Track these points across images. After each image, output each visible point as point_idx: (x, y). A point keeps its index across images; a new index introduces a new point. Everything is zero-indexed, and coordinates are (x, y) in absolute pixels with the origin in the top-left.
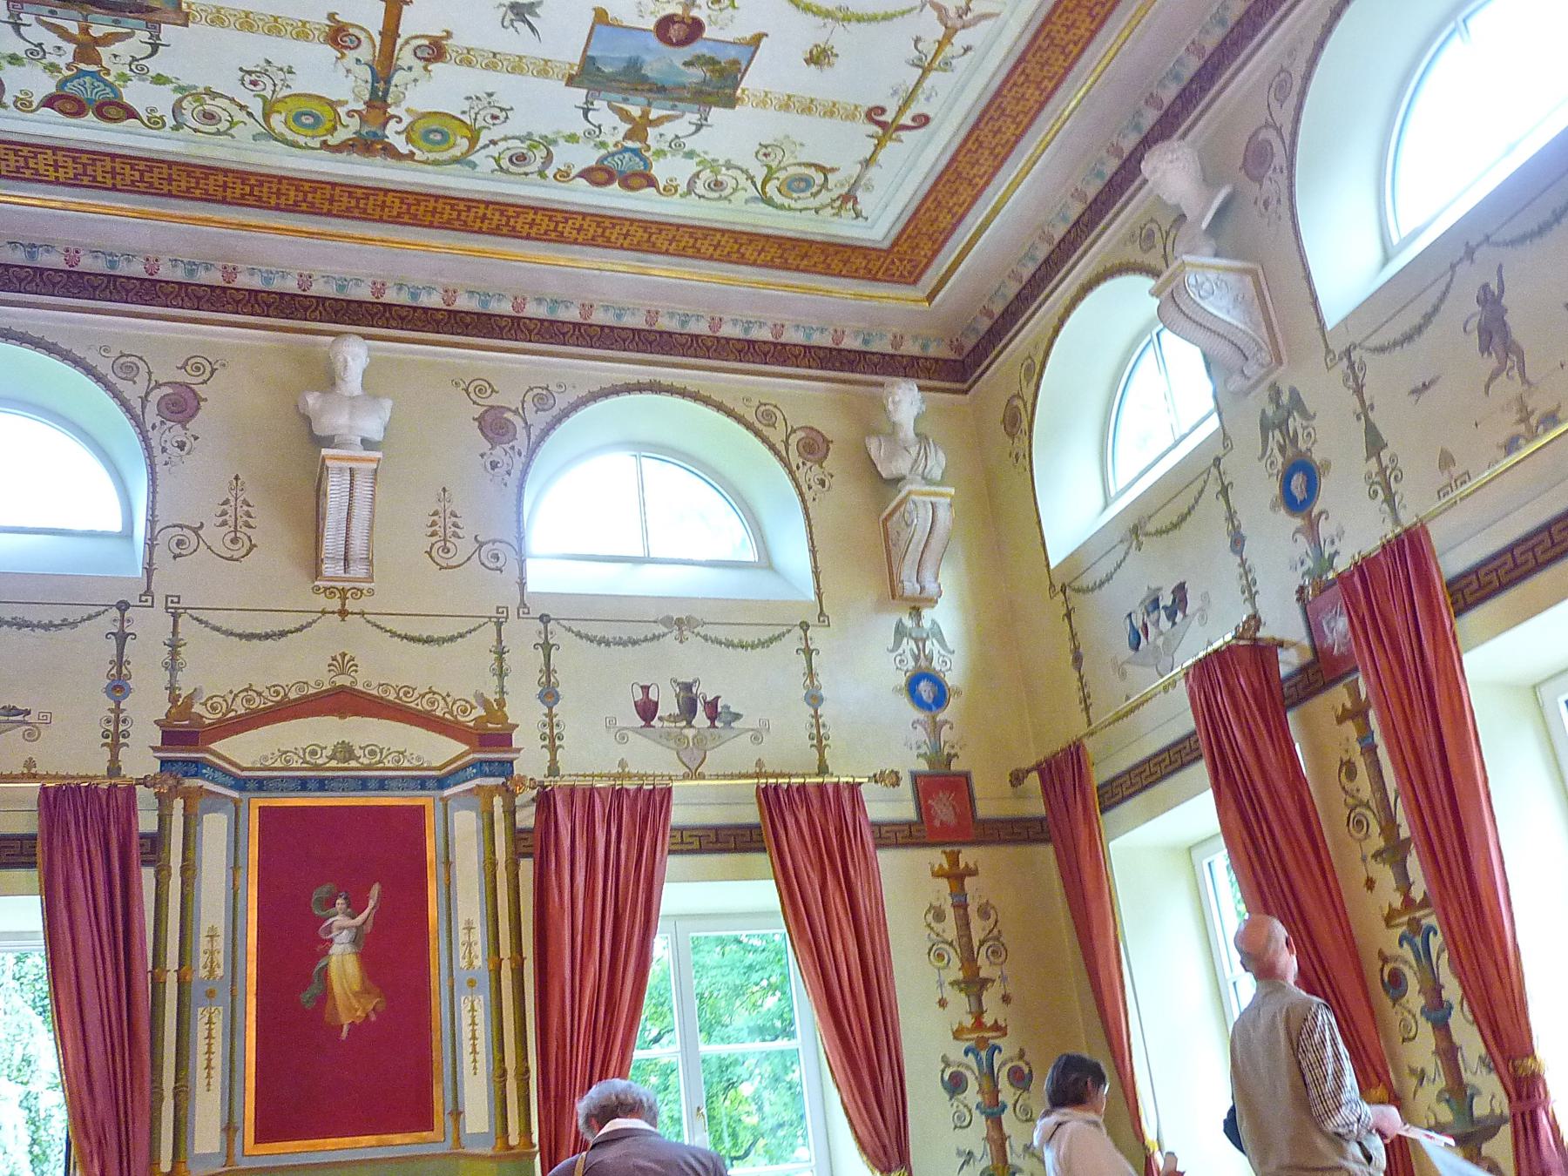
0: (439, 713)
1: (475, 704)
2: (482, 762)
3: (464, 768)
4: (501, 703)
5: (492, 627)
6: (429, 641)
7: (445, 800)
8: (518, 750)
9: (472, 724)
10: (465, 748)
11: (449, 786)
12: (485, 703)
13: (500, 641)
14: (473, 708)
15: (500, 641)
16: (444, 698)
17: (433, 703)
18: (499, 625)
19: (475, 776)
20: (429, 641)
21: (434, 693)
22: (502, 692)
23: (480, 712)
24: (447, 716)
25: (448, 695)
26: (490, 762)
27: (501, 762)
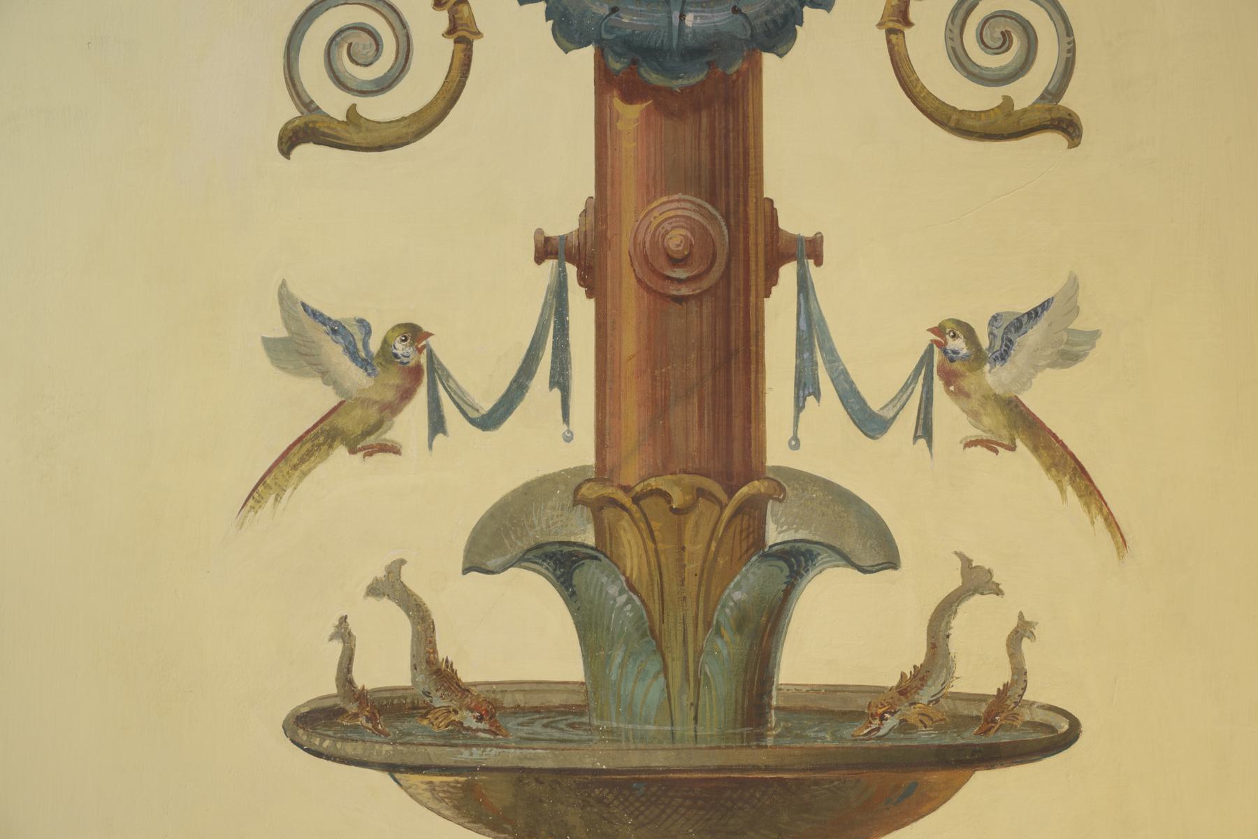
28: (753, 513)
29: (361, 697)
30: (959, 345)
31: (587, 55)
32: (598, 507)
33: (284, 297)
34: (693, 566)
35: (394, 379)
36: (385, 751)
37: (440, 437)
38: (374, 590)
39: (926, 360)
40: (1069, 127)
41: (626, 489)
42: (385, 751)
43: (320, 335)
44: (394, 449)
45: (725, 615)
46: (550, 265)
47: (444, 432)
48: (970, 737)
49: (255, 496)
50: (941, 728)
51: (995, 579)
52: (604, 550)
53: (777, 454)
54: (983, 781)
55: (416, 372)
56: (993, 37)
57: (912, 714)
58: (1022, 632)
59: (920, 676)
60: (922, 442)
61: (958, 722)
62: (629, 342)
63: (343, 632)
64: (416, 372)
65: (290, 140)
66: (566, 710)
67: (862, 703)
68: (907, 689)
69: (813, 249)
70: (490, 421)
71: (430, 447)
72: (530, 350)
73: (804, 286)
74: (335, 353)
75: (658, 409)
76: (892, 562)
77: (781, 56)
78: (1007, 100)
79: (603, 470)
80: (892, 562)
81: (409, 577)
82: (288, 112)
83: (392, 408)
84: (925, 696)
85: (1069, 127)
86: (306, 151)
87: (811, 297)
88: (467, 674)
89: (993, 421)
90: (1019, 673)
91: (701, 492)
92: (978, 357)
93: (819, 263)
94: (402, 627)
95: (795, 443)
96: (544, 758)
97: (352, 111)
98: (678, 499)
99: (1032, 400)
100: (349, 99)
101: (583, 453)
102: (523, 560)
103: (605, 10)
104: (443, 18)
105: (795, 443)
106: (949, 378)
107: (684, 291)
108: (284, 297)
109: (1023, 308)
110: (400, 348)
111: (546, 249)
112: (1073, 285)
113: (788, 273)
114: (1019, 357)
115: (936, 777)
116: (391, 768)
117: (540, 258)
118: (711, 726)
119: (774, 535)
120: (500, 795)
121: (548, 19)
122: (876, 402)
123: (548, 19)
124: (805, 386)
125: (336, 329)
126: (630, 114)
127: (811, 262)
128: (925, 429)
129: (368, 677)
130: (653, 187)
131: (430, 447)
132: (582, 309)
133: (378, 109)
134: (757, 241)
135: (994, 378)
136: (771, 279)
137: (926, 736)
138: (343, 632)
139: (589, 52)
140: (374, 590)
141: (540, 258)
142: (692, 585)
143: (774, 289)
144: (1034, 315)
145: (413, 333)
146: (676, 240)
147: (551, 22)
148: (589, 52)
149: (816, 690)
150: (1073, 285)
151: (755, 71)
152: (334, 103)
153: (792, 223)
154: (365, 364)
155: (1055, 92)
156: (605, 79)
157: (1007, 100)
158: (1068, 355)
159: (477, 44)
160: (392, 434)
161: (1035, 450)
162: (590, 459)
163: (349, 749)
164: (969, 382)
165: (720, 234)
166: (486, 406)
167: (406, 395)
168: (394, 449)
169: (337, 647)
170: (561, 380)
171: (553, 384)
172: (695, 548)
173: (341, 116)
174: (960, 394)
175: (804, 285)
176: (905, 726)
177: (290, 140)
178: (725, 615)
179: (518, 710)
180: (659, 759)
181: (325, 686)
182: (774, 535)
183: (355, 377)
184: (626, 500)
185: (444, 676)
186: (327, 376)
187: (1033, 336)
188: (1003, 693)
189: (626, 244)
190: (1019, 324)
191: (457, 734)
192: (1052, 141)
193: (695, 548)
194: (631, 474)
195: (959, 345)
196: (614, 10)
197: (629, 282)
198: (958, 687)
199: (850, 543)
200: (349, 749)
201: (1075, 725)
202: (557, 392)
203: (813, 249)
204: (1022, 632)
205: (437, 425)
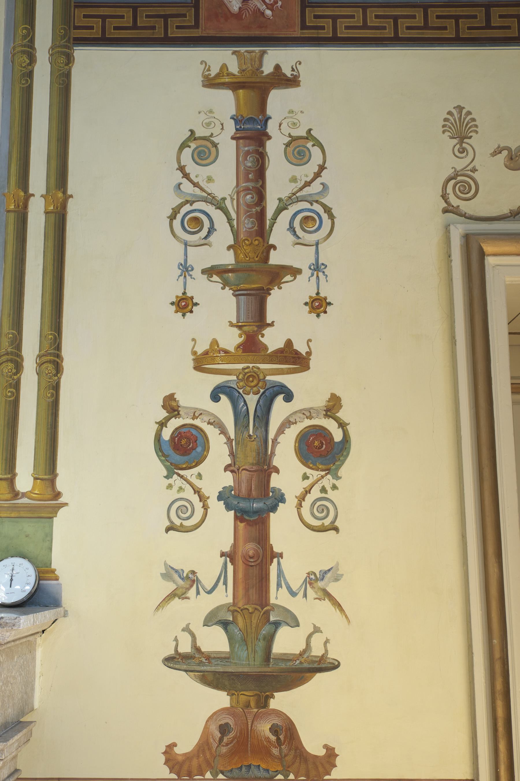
28: (267, 614)
29: (180, 654)
30: (313, 577)
31: (232, 512)
32: (233, 612)
33: (165, 564)
34: (254, 626)
35: (189, 582)
36: (185, 667)
37: (199, 595)
38: (183, 630)
39: (305, 580)
40: (336, 529)
41: (239, 608)
42: (185, 667)
43: (173, 572)
44: (188, 598)
45: (261, 637)
46: (223, 558)
47: (200, 595)
48: (316, 665)
49: (157, 608)
50: (309, 663)
51: (321, 629)
52: (234, 622)
53: (273, 600)
54: (319, 676)
55: (193, 581)
56: (320, 510)
57: (303, 660)
58: (327, 641)
59: (305, 651)
60: (305, 598)
61: (314, 662)
62: (240, 575)
63: (176, 640)
64: (193, 581)
65: (168, 530)
66: (225, 658)
67: (291, 657)
68: (301, 654)
69: (281, 555)
70: (210, 592)
71: (196, 598)
72: (219, 576)
73: (279, 563)
74: (176, 577)
75: (247, 590)
76: (298, 625)
77: (274, 513)
78: (323, 523)
79: (234, 604)
80: (298, 625)
81: (191, 627)
82: (168, 524)
83: (188, 589)
84: (305, 656)
85: (336, 529)
86: (171, 532)
87: (280, 566)
88: (203, 650)
89: (320, 594)
90: (326, 651)
91: (256, 609)
92: (317, 580)
93: (282, 558)
94: (189, 638)
95: (277, 598)
96: (220, 669)
97: (181, 523)
98: (251, 610)
99: (329, 589)
100: (180, 521)
101: (230, 600)
102: (216, 624)
103: (236, 503)
104: (201, 504)
105: (277, 598)
106: (311, 584)
107: (253, 564)
108: (165, 564)
109: (327, 569)
110: (190, 576)
111: (223, 554)
112: (338, 564)
113: (275, 560)
114: (326, 580)
115: (308, 675)
116: (186, 671)
117: (221, 557)
118: (257, 663)
119: (272, 619)
120: (210, 677)
121: (222, 488)
122: (294, 589)
123: (222, 488)
124: (279, 585)
125: (176, 571)
126: (241, 525)
127: (280, 558)
128: (305, 595)
129: (181, 650)
130: (246, 541)
131: (196, 598)
132: (230, 568)
133: (187, 523)
134: (269, 553)
135: (320, 584)
136: (272, 562)
137: (306, 665)
138: (176, 640)
139: (233, 512)
140: (183, 630)
141: (221, 557)
142: (254, 629)
143: (272, 564)
144: (329, 570)
145: (193, 572)
146: (251, 553)
147: (225, 505)
148: (233, 512)
149: (281, 654)
150: (338, 564)
151: (269, 516)
152: (177, 522)
153: (276, 549)
154: (183, 579)
155: (333, 522)
156: (236, 518)
157: (323, 523)
158: (337, 580)
159: (209, 510)
160: (188, 595)
161: (329, 600)
162: (231, 601)
163: (176, 666)
164: (315, 585)
165: (261, 552)
166: (209, 589)
167: (191, 586)
168: (188, 598)
169: (175, 643)
170: (225, 583)
171: (223, 584)
172: (254, 621)
173: (179, 525)
174: (313, 588)
175: (279, 563)
176: (301, 663)
177: (168, 530)
178: (261, 637)
179: (214, 658)
180: (246, 670)
181: (171, 652)
182: (272, 619)
183: (180, 582)
184: (239, 610)
185: (198, 650)
186: (174, 581)
187: (329, 575)
188: (323, 656)
189: (240, 554)
190: (326, 572)
191: (201, 663)
192: (333, 532)
193: (254, 621)
194: (240, 604)
195: (313, 577)
196: (238, 503)
197: (241, 562)
198: (313, 654)
199: (289, 621)
200: (176, 666)
201: (339, 663)
202: (224, 586)
203: (281, 555)
204: (327, 641)
205: (198, 593)
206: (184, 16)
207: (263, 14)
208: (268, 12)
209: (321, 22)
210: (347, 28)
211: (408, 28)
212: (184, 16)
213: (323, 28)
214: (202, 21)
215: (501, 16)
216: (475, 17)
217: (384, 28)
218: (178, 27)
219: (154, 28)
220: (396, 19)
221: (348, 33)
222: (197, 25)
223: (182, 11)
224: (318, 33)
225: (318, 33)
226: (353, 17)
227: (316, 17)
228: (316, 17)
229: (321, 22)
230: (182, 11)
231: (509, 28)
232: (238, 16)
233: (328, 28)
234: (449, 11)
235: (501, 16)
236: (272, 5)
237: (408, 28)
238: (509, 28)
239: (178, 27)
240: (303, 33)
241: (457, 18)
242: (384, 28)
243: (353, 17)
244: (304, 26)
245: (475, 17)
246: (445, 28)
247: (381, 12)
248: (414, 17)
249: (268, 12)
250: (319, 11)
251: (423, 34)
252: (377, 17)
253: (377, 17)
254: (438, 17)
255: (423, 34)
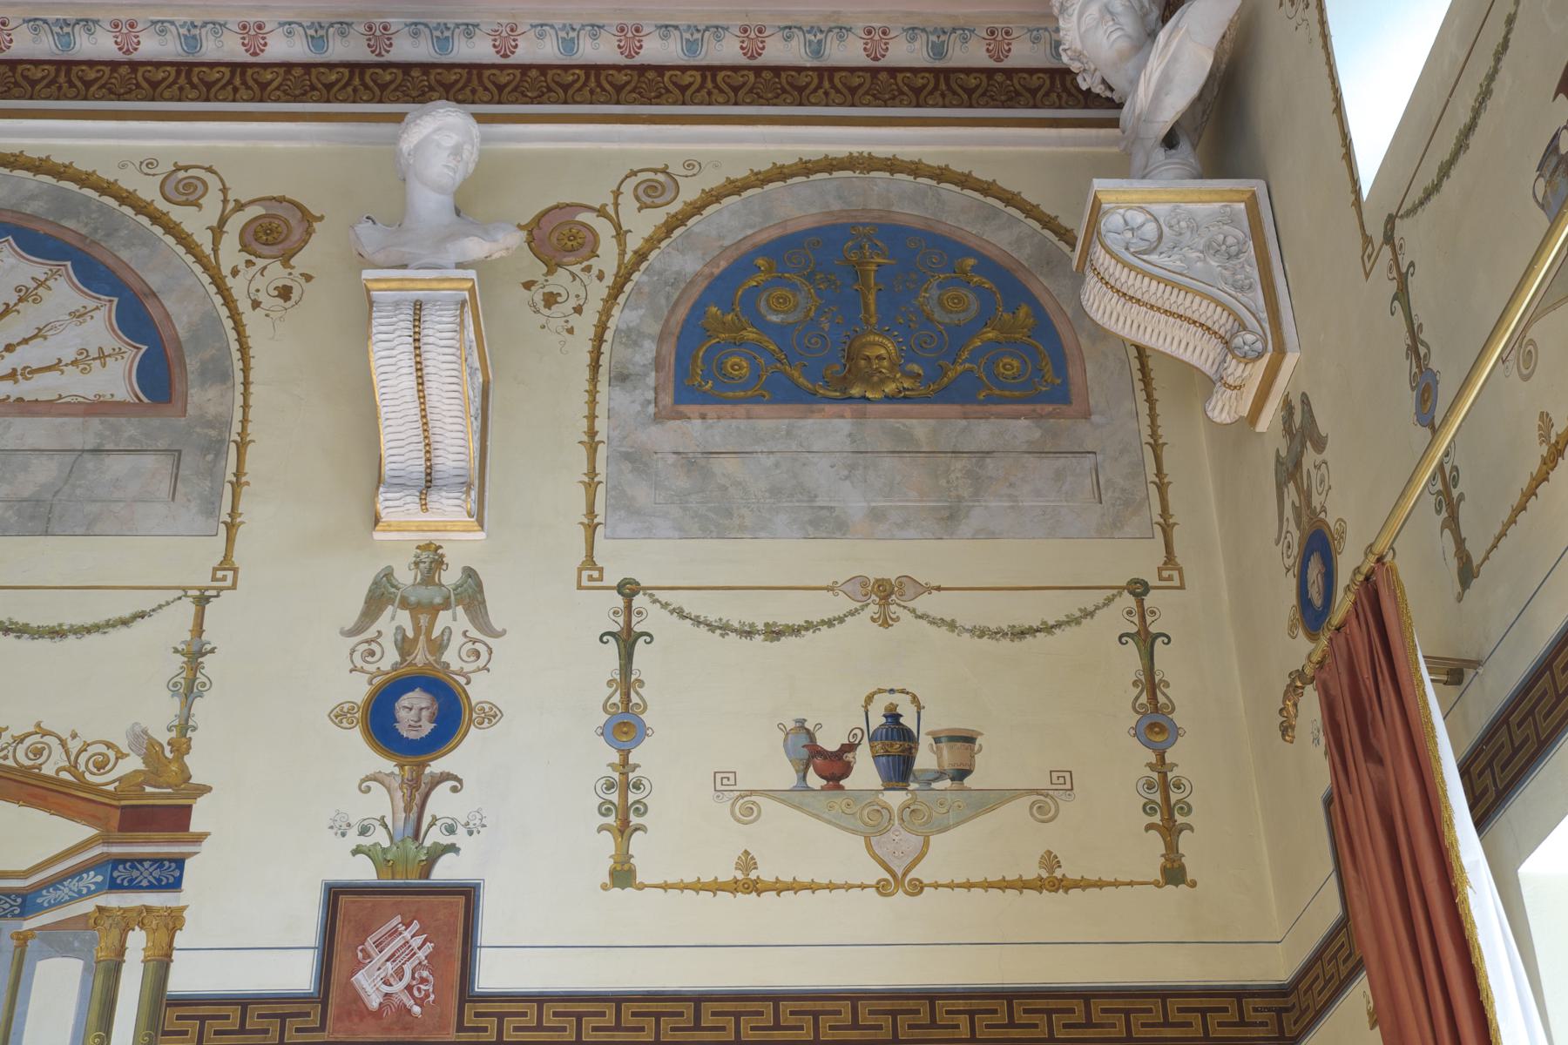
0: (49, 770)
1: (125, 750)
2: (117, 862)
3: (76, 873)
4: (181, 746)
5: (188, 608)
6: (57, 633)
7: (23, 939)
8: (199, 838)
9: (111, 788)
10: (86, 832)
11: (40, 909)
12: (151, 750)
13: (199, 629)
14: (121, 756)
15: (199, 629)
16: (63, 743)
17: (38, 753)
18: (202, 601)
19: (99, 889)
20: (57, 633)
21: (46, 733)
22: (184, 727)
23: (134, 763)
24: (65, 776)
25: (74, 736)
26: (136, 861)
27: (158, 861)
206: (308, 1015)
207: (409, 1011)
208: (417, 1009)
209: (483, 1022)
210: (516, 1029)
211: (595, 1029)
212: (308, 1015)
213: (485, 1029)
214: (330, 1023)
215: (714, 1014)
216: (681, 1014)
217: (564, 1029)
218: (298, 1030)
219: (266, 1031)
220: (579, 1017)
221: (517, 1036)
222: (322, 1028)
223: (306, 1008)
224: (478, 1037)
225: (478, 1037)
226: (524, 1014)
227: (477, 1015)
228: (477, 1015)
229: (483, 1022)
230: (306, 1008)
231: (723, 1029)
232: (378, 1014)
233: (492, 1030)
234: (648, 1007)
235: (714, 1014)
236: (422, 999)
237: (595, 1029)
238: (723, 1029)
239: (298, 1030)
240: (458, 1037)
241: (658, 1016)
242: (564, 1029)
243: (524, 1014)
244: (461, 1028)
245: (681, 1014)
246: (642, 1029)
247: (560, 1008)
248: (603, 1014)
249: (417, 1009)
250: (482, 1007)
251: (613, 1036)
252: (556, 1014)
253: (556, 1014)
254: (634, 1014)
255: (613, 1036)
